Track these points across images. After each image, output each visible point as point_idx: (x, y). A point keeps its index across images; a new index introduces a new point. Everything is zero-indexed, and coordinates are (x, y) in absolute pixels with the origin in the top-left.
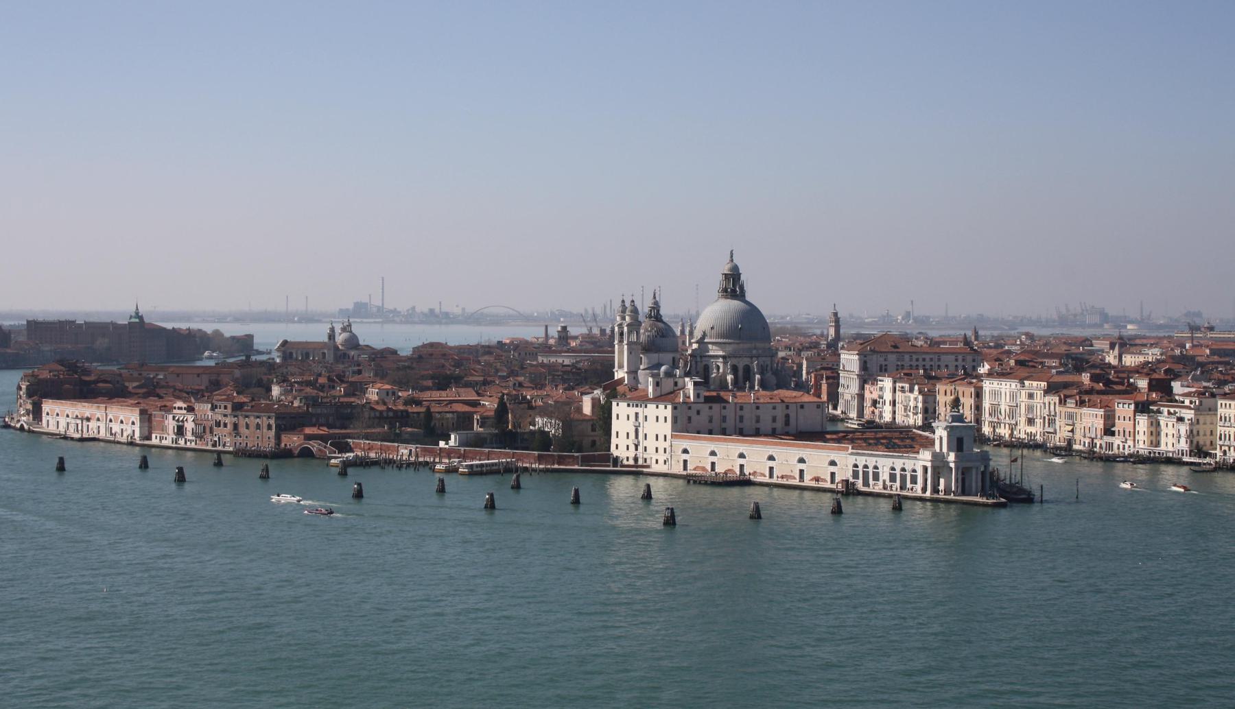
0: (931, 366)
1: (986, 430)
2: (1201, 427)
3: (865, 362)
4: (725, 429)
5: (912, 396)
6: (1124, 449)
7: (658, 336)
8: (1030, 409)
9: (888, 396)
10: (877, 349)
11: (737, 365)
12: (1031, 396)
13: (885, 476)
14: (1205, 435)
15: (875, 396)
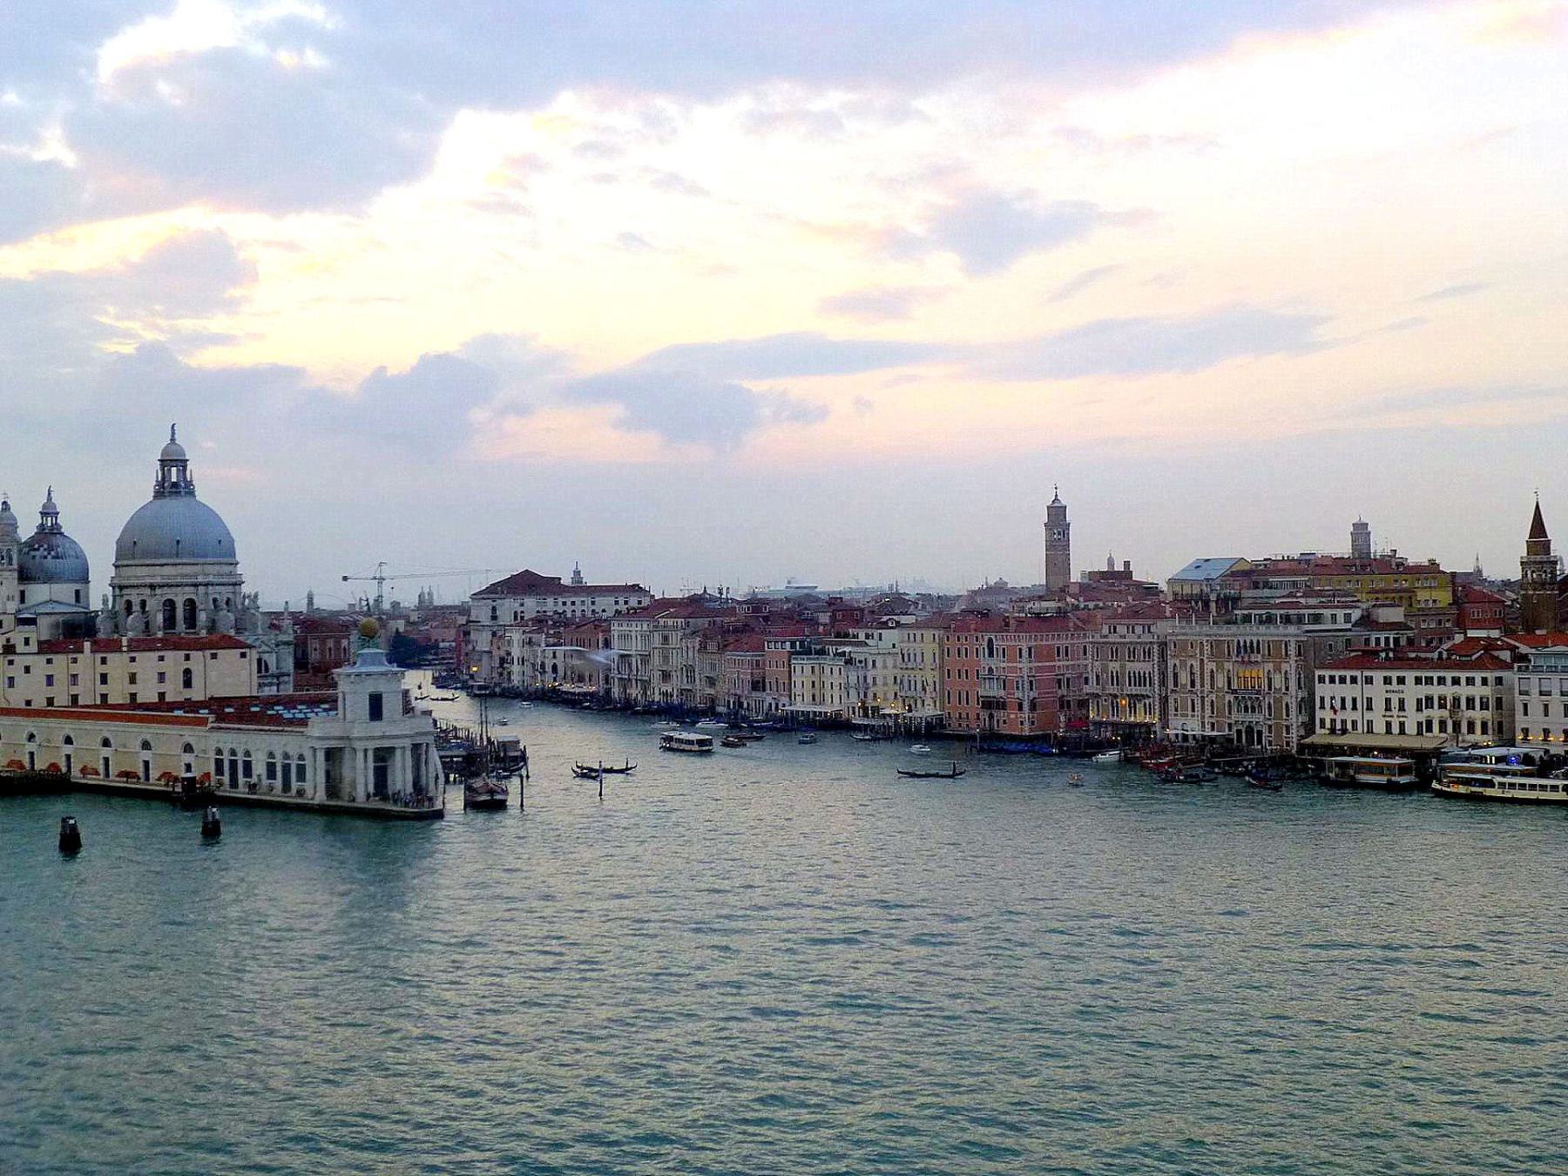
0: (574, 611)
1: (616, 691)
2: (879, 672)
3: (494, 609)
4: (77, 696)
6: (777, 708)
9: (516, 652)
11: (174, 599)
12: (666, 638)
13: (259, 769)
14: (885, 684)
15: (503, 653)
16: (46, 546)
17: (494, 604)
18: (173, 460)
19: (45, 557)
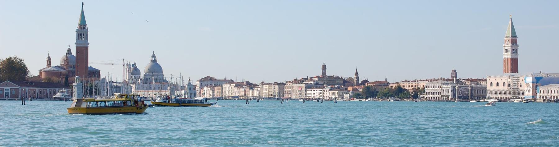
3: (201, 83)
5: (210, 91)
8: (232, 91)
12: (232, 88)
18: (154, 56)
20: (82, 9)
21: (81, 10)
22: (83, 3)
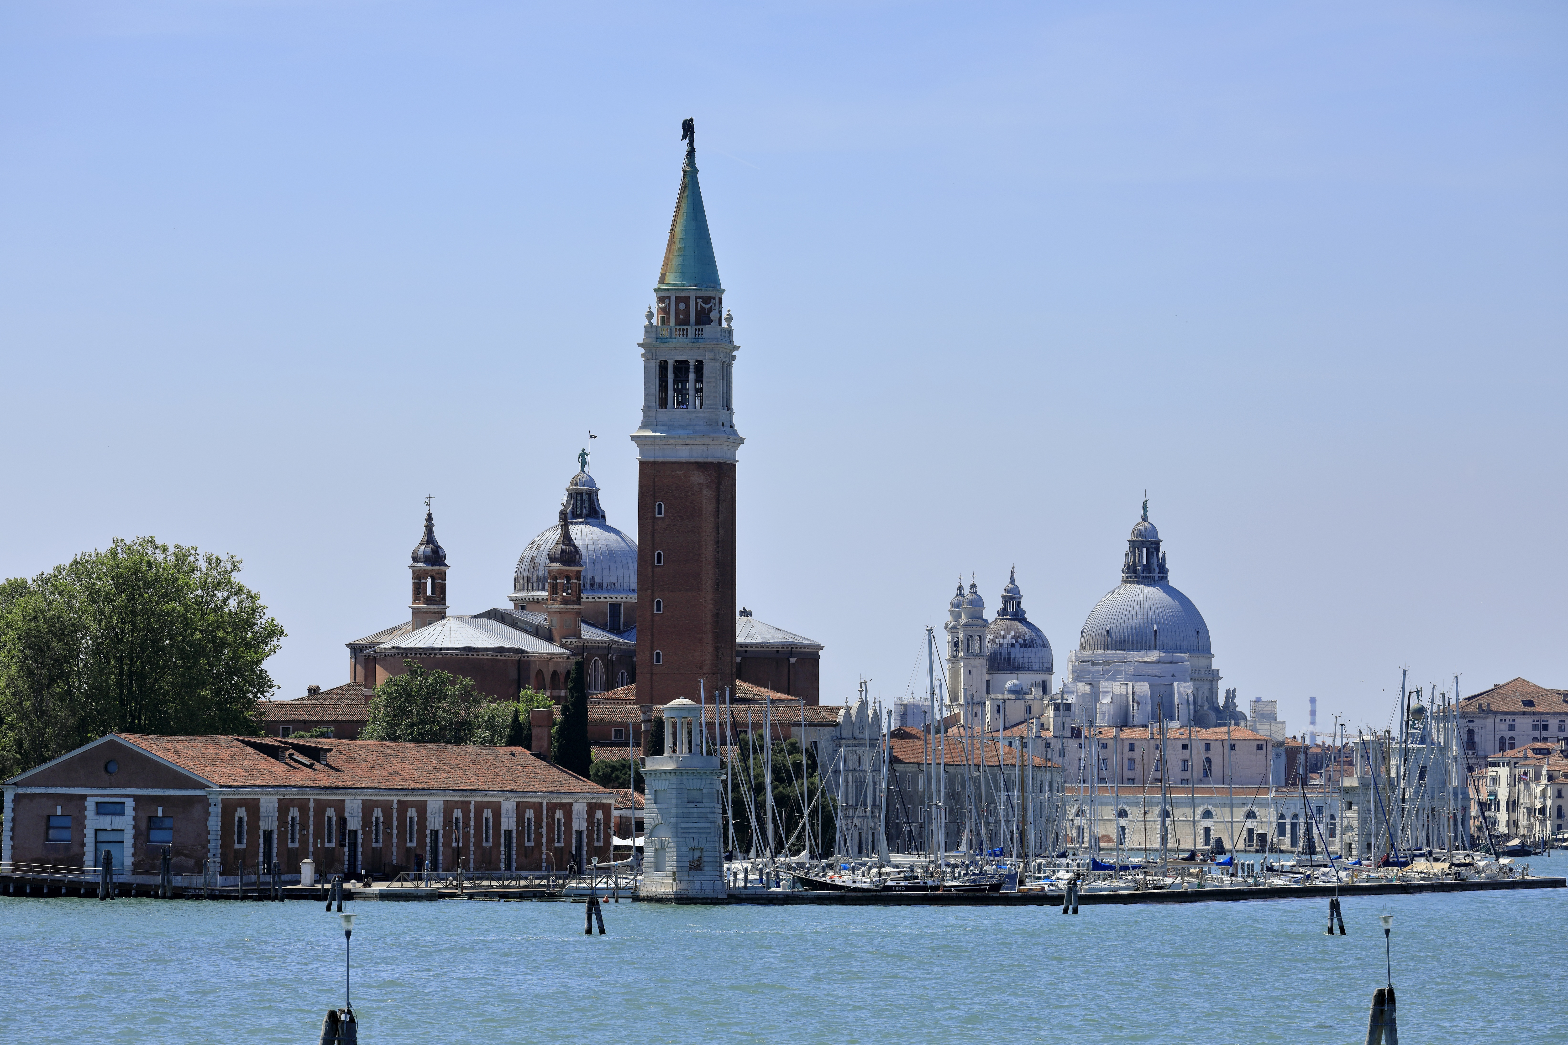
3: (1471, 732)
7: (1017, 645)
10: (1494, 707)
16: (1012, 633)
17: (1471, 725)
19: (1013, 645)
20: (691, 173)
21: (676, 180)
22: (688, 128)
